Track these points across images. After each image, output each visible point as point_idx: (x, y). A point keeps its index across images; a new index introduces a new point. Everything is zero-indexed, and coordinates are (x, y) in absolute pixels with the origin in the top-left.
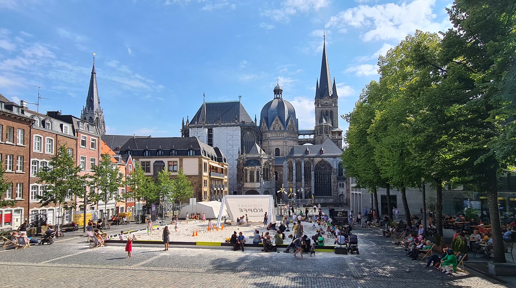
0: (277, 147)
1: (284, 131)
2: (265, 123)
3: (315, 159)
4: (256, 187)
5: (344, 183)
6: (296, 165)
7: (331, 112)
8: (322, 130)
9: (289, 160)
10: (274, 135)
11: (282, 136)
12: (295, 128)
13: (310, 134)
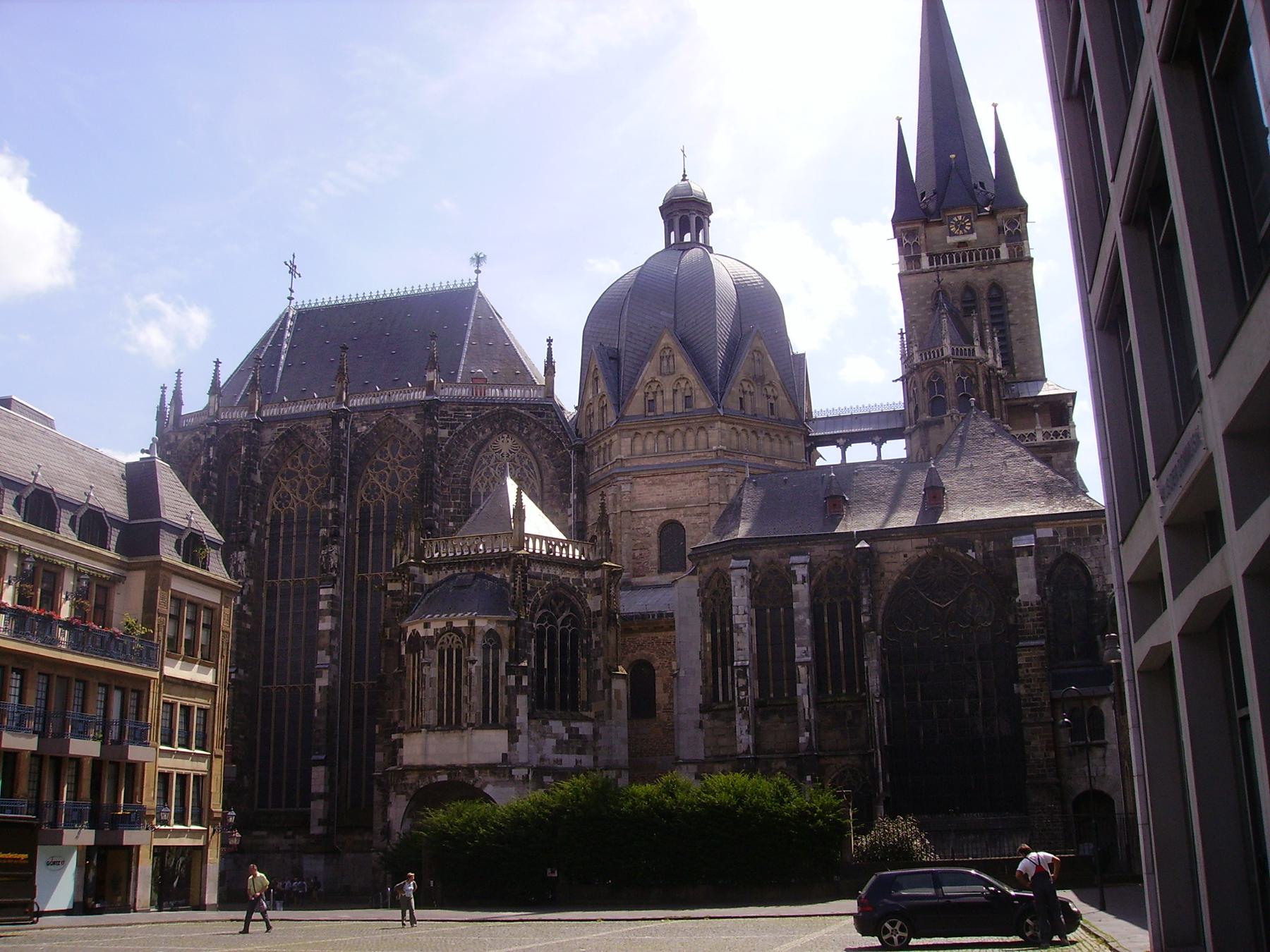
0: (667, 516)
1: (712, 415)
2: (601, 382)
3: (883, 546)
4: (476, 759)
5: (1106, 707)
6: (757, 595)
7: (994, 293)
8: (942, 385)
9: (706, 569)
10: (650, 442)
11: (702, 445)
12: (782, 398)
13: (879, 437)
